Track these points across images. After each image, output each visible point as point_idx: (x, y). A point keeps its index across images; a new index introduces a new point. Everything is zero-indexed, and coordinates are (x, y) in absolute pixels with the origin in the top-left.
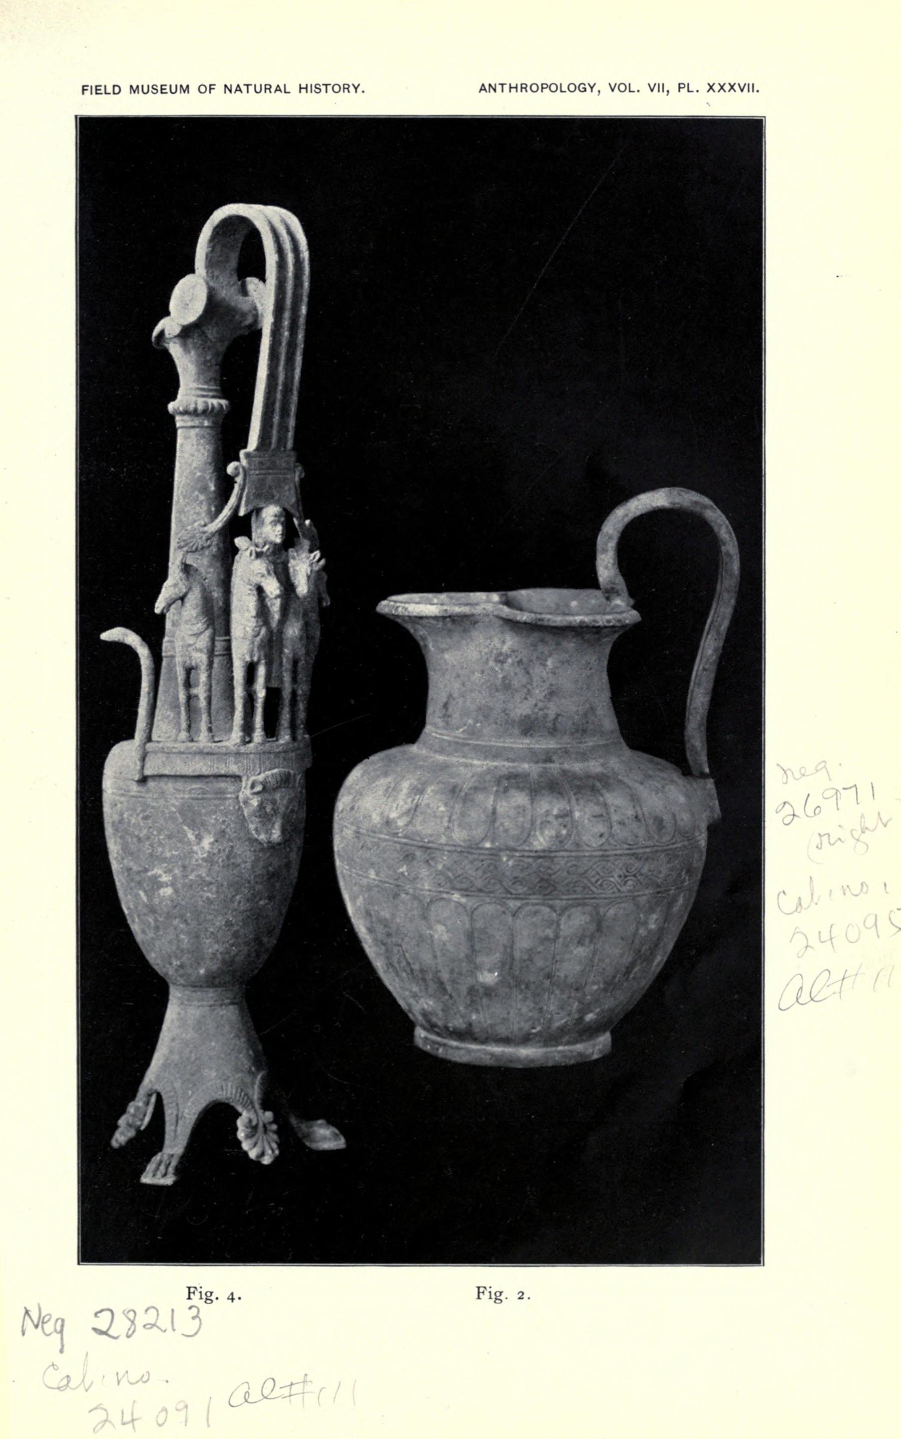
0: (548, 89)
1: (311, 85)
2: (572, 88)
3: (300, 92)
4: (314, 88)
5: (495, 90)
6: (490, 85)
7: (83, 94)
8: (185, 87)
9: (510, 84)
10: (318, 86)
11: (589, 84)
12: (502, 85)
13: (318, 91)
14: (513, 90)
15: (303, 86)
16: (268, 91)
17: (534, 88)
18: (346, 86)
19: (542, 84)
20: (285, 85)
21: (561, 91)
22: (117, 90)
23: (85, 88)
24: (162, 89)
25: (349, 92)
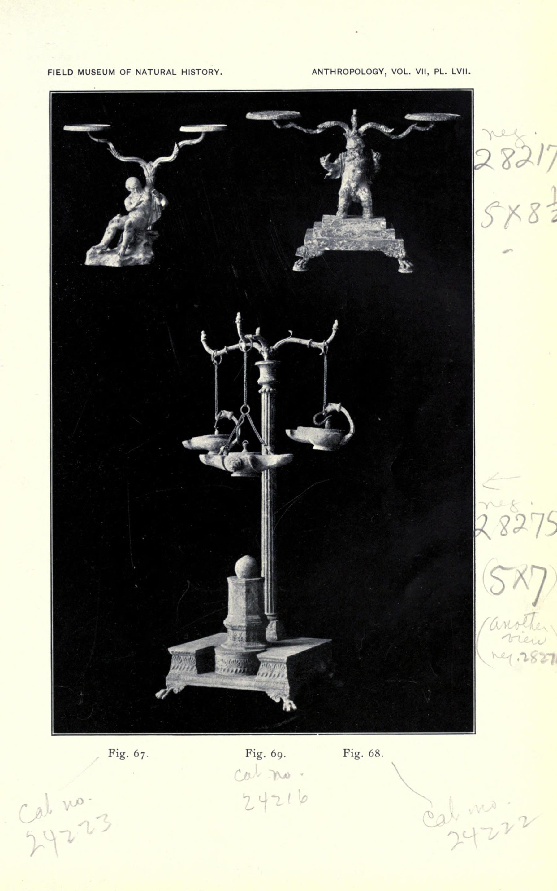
0: (354, 72)
1: (189, 70)
2: (369, 72)
3: (182, 74)
4: (190, 72)
5: (322, 73)
6: (319, 70)
7: (49, 75)
8: (112, 71)
9: (331, 70)
10: (193, 71)
11: (379, 69)
12: (326, 70)
14: (333, 73)
15: (184, 70)
16: (163, 73)
17: (346, 72)
18: (211, 71)
19: (351, 70)
20: (173, 70)
21: (362, 74)
22: (70, 72)
23: (50, 71)
24: (98, 72)
25: (212, 74)
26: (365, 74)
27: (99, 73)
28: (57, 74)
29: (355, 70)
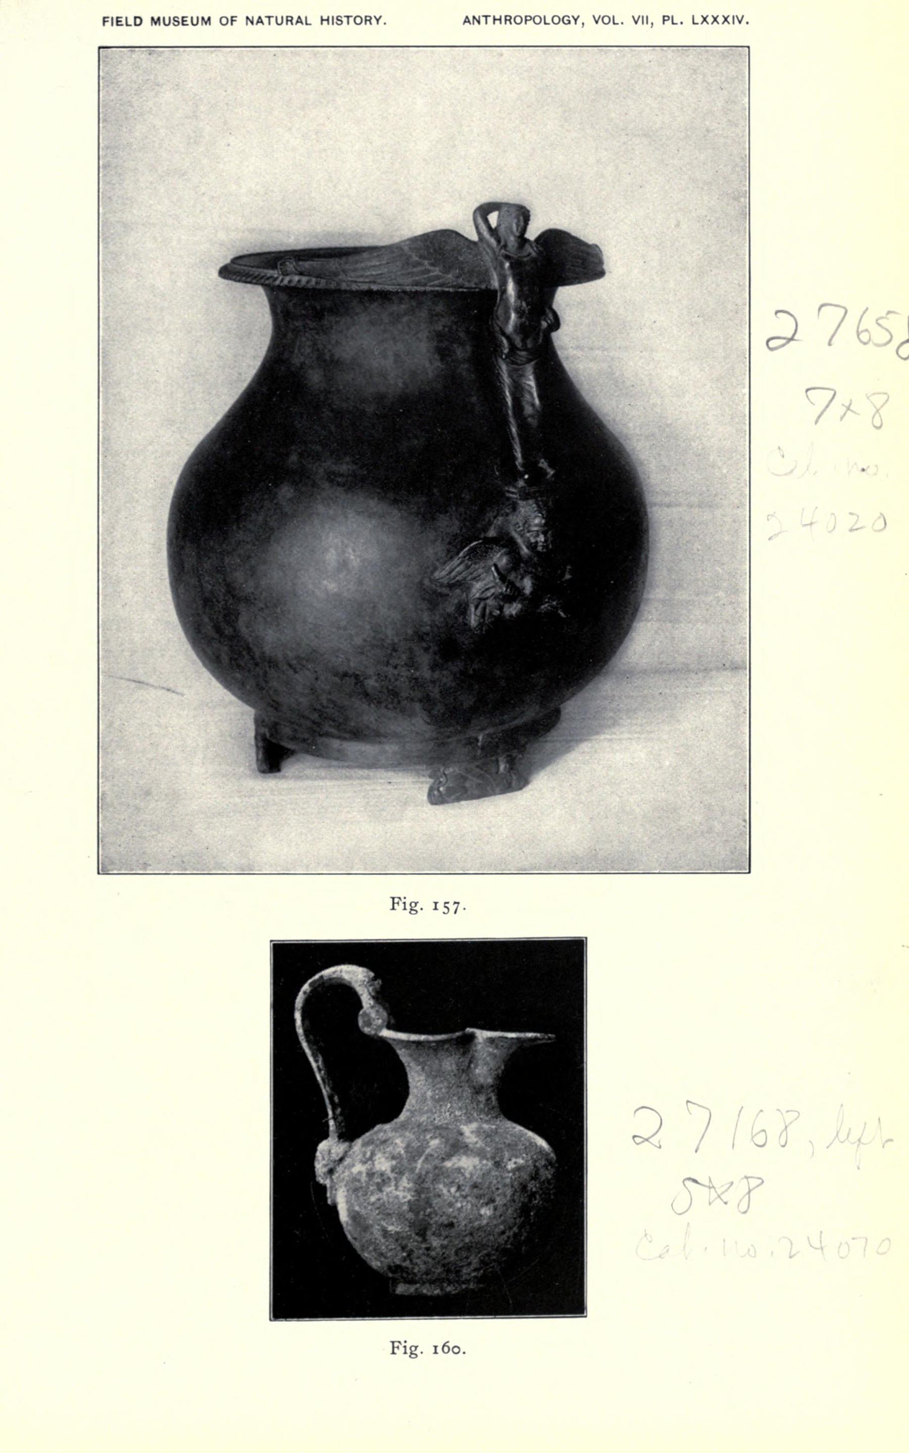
0: (532, 21)
1: (333, 17)
2: (556, 20)
3: (322, 24)
4: (335, 20)
5: (479, 22)
6: (474, 17)
7: (104, 25)
8: (206, 19)
9: (494, 17)
10: (339, 18)
11: (573, 17)
12: (486, 17)
13: (339, 22)
14: (497, 22)
15: (325, 17)
16: (289, 23)
17: (518, 20)
18: (368, 18)
19: (526, 17)
20: (306, 18)
22: (138, 21)
23: (106, 20)
24: (183, 21)
25: (371, 24)
26: (549, 24)
27: (185, 23)
28: (117, 25)
29: (561, 18)
